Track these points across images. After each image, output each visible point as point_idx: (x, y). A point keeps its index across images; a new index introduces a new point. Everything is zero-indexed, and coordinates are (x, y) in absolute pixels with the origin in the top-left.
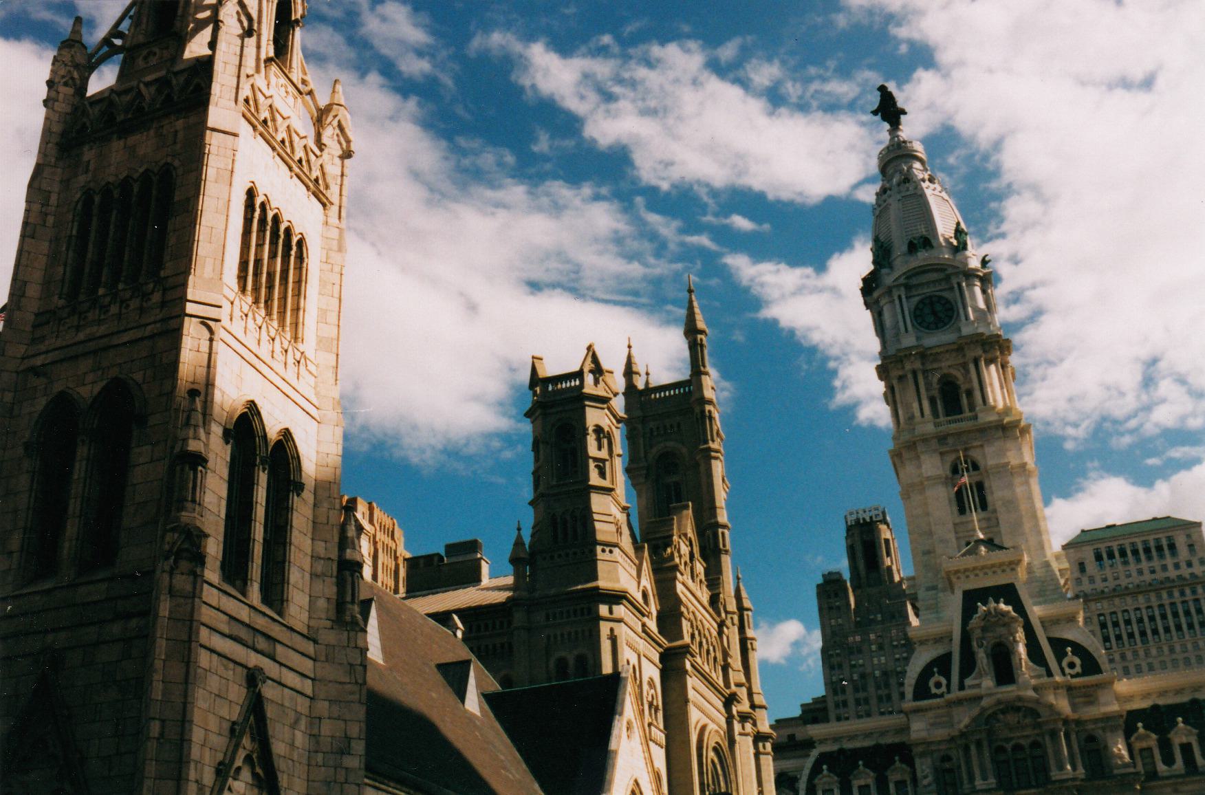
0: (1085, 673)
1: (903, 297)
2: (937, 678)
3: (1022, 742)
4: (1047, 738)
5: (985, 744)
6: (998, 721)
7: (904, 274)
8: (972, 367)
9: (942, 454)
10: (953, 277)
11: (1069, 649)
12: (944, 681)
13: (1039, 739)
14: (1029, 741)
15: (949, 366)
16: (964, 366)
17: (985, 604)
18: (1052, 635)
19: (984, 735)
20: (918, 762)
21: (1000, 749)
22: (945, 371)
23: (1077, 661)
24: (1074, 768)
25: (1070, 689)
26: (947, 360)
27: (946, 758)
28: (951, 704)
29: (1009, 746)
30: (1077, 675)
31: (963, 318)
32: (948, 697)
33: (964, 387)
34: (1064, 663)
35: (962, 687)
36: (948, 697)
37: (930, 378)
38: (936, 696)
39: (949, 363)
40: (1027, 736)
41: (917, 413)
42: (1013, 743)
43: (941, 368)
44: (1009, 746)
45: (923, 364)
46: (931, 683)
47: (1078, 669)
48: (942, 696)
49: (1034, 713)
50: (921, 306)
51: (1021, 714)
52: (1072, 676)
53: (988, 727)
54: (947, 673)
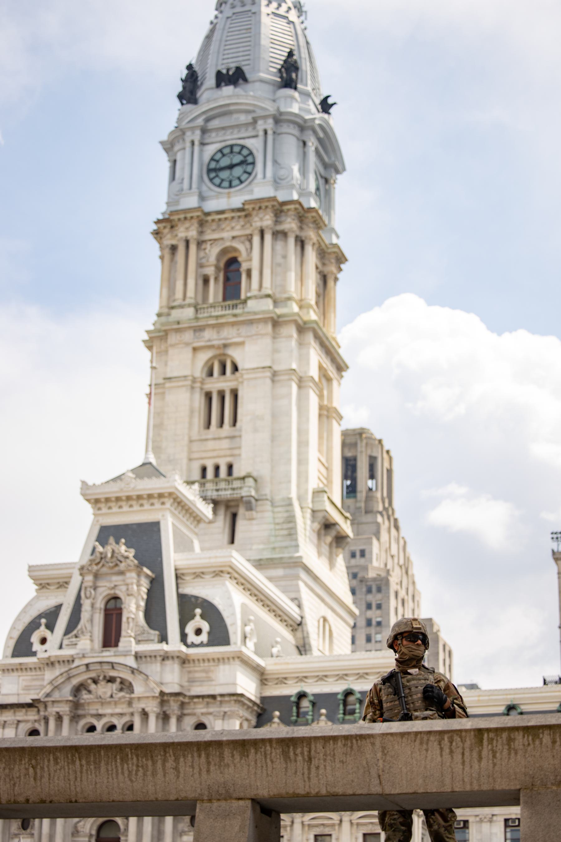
0: (211, 643)
1: (197, 143)
3: (115, 721)
6: (90, 692)
7: (204, 113)
8: (256, 240)
9: (195, 349)
10: (260, 122)
11: (198, 611)
15: (234, 238)
16: (249, 238)
19: (64, 709)
22: (228, 244)
23: (205, 627)
26: (233, 228)
30: (201, 645)
31: (260, 176)
33: (244, 266)
34: (190, 629)
37: (207, 251)
39: (235, 233)
40: (122, 714)
41: (179, 294)
42: (104, 720)
43: (222, 239)
44: (99, 726)
45: (201, 233)
46: (35, 638)
47: (204, 637)
49: (125, 686)
50: (219, 156)
51: (115, 686)
52: (193, 645)
54: (51, 627)
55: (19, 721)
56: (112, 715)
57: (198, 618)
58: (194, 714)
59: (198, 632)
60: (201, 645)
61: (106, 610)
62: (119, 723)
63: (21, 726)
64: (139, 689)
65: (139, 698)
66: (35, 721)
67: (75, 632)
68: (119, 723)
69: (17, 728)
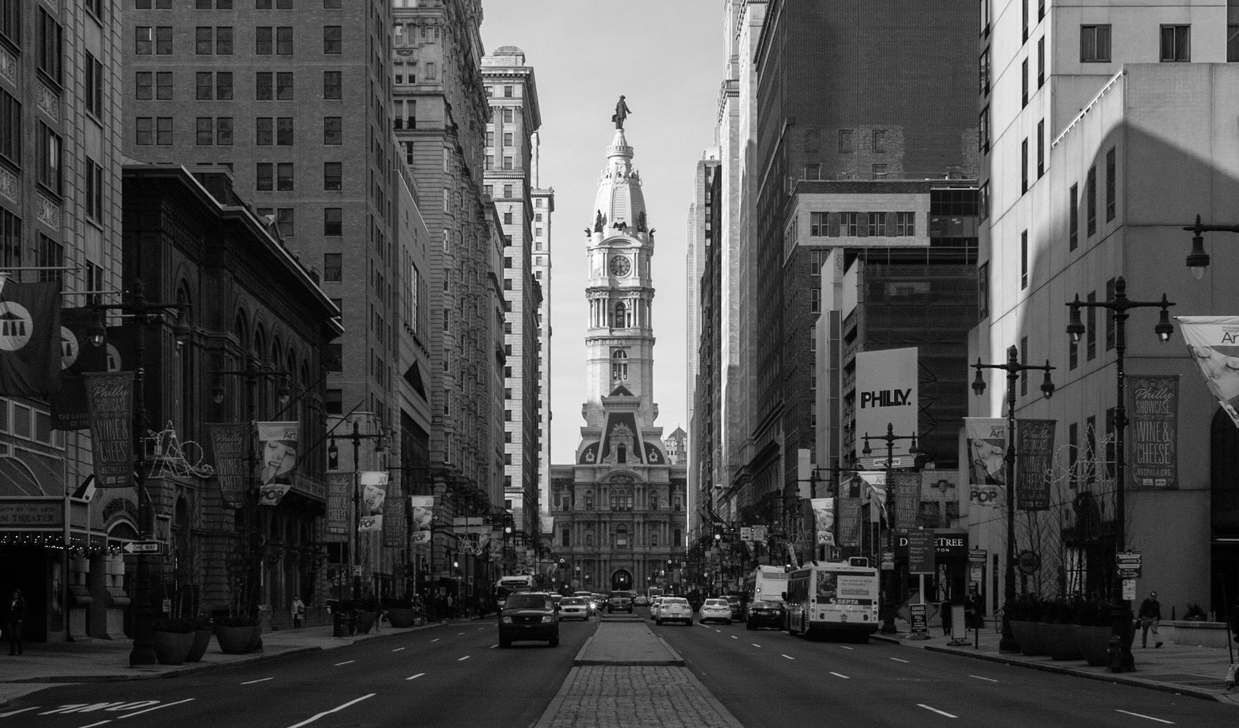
12: (593, 456)
18: (646, 441)
20: (577, 492)
24: (644, 506)
25: (650, 469)
27: (589, 492)
28: (594, 469)
29: (618, 491)
30: (655, 463)
32: (594, 465)
36: (594, 465)
38: (588, 463)
44: (618, 491)
46: (587, 456)
47: (656, 460)
48: (591, 463)
52: (652, 463)
54: (595, 452)
59: (653, 457)
60: (655, 463)
62: (626, 491)
64: (636, 481)
68: (626, 491)
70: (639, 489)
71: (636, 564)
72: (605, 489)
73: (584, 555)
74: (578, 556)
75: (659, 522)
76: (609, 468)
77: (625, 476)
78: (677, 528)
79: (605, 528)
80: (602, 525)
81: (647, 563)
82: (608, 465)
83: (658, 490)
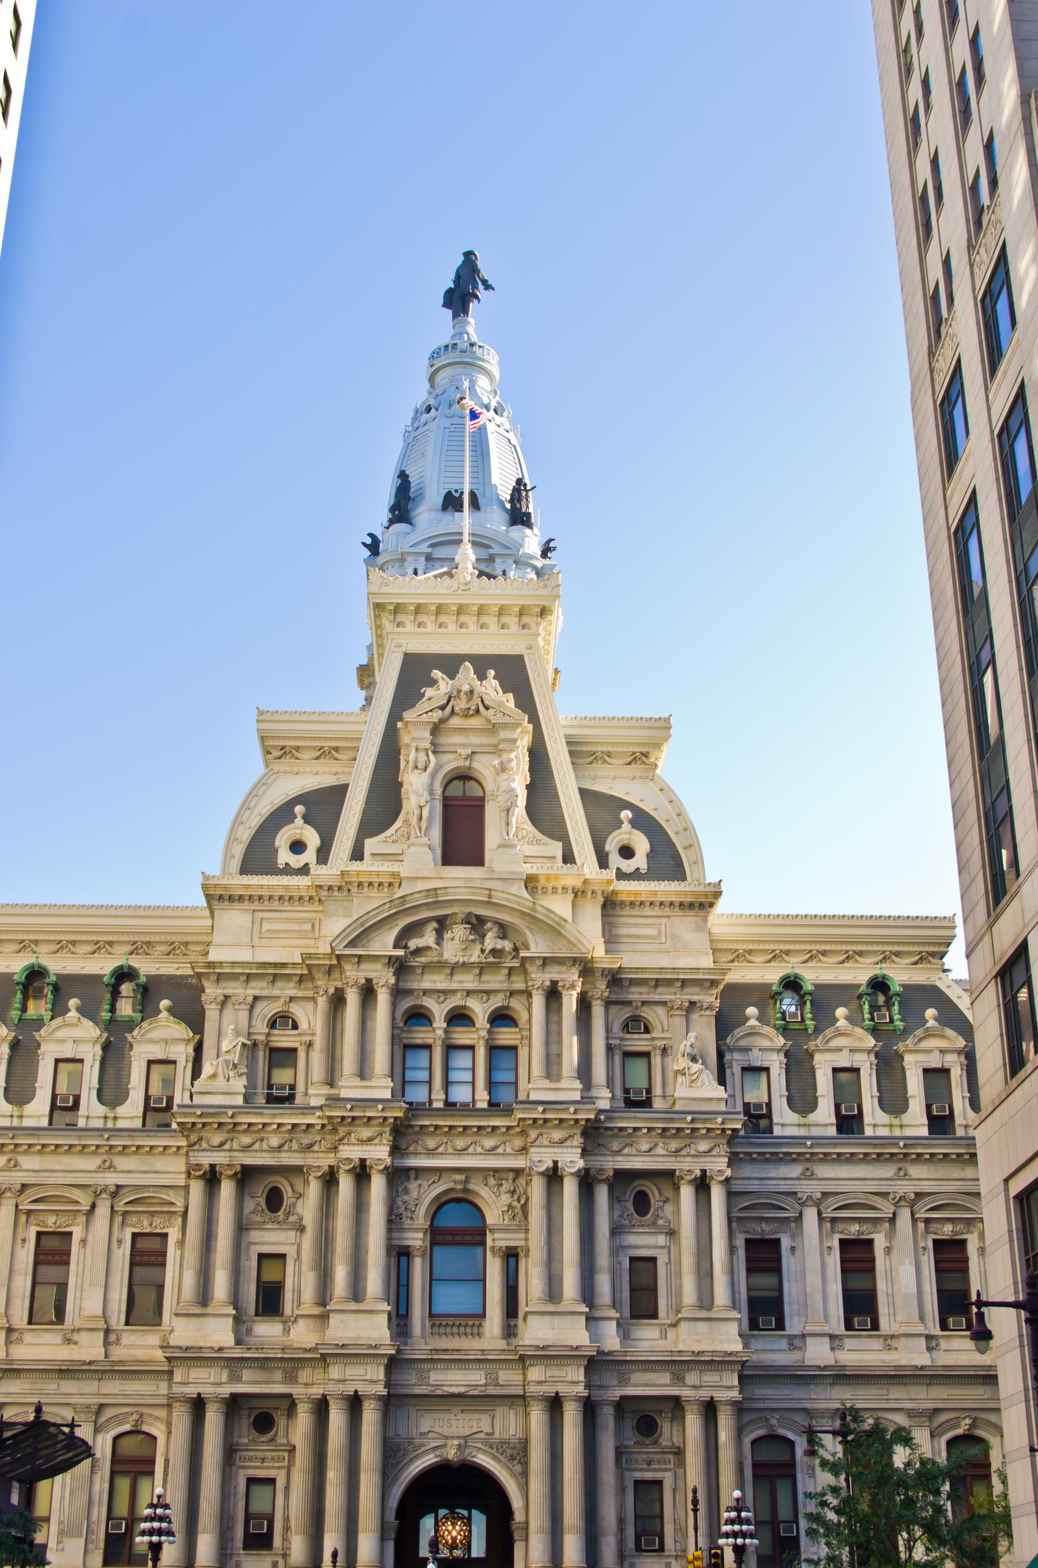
0: (652, 874)
2: (300, 829)
4: (538, 1001)
5: (383, 998)
13: (517, 1005)
14: (497, 1001)
17: (452, 674)
21: (419, 1016)
23: (641, 844)
27: (282, 1020)
29: (439, 1011)
35: (357, 854)
44: (439, 1011)
48: (304, 870)
52: (621, 875)
53: (400, 952)
55: (256, 998)
56: (469, 993)
57: (626, 826)
58: (629, 1003)
60: (636, 875)
61: (445, 799)
62: (480, 1010)
63: (260, 1006)
65: (546, 962)
66: (291, 999)
67: (391, 831)
68: (480, 1010)
69: (251, 1011)
70: (553, 995)
71: (538, 1418)
72: (368, 992)
73: (235, 1365)
74: (197, 1374)
75: (668, 1177)
76: (395, 881)
77: (477, 925)
78: (766, 1230)
79: (360, 1207)
80: (346, 1185)
81: (607, 1417)
82: (387, 867)
83: (656, 1016)
